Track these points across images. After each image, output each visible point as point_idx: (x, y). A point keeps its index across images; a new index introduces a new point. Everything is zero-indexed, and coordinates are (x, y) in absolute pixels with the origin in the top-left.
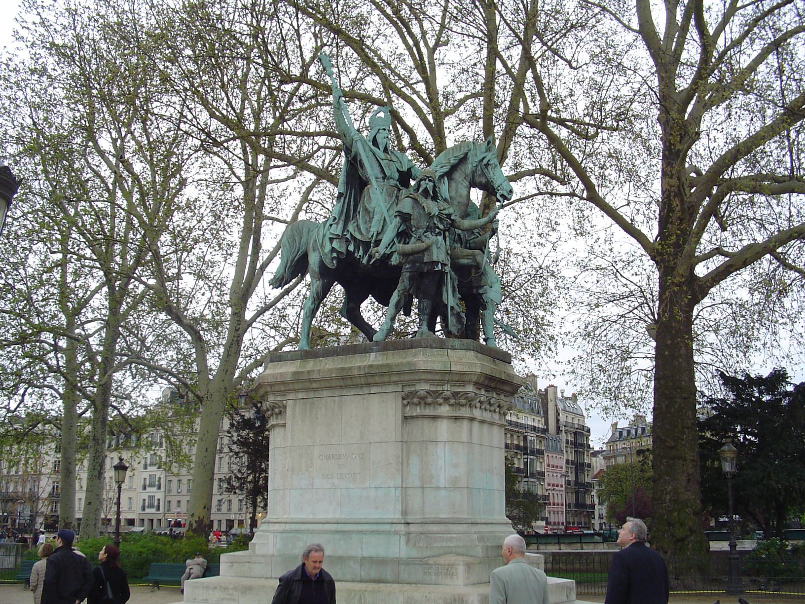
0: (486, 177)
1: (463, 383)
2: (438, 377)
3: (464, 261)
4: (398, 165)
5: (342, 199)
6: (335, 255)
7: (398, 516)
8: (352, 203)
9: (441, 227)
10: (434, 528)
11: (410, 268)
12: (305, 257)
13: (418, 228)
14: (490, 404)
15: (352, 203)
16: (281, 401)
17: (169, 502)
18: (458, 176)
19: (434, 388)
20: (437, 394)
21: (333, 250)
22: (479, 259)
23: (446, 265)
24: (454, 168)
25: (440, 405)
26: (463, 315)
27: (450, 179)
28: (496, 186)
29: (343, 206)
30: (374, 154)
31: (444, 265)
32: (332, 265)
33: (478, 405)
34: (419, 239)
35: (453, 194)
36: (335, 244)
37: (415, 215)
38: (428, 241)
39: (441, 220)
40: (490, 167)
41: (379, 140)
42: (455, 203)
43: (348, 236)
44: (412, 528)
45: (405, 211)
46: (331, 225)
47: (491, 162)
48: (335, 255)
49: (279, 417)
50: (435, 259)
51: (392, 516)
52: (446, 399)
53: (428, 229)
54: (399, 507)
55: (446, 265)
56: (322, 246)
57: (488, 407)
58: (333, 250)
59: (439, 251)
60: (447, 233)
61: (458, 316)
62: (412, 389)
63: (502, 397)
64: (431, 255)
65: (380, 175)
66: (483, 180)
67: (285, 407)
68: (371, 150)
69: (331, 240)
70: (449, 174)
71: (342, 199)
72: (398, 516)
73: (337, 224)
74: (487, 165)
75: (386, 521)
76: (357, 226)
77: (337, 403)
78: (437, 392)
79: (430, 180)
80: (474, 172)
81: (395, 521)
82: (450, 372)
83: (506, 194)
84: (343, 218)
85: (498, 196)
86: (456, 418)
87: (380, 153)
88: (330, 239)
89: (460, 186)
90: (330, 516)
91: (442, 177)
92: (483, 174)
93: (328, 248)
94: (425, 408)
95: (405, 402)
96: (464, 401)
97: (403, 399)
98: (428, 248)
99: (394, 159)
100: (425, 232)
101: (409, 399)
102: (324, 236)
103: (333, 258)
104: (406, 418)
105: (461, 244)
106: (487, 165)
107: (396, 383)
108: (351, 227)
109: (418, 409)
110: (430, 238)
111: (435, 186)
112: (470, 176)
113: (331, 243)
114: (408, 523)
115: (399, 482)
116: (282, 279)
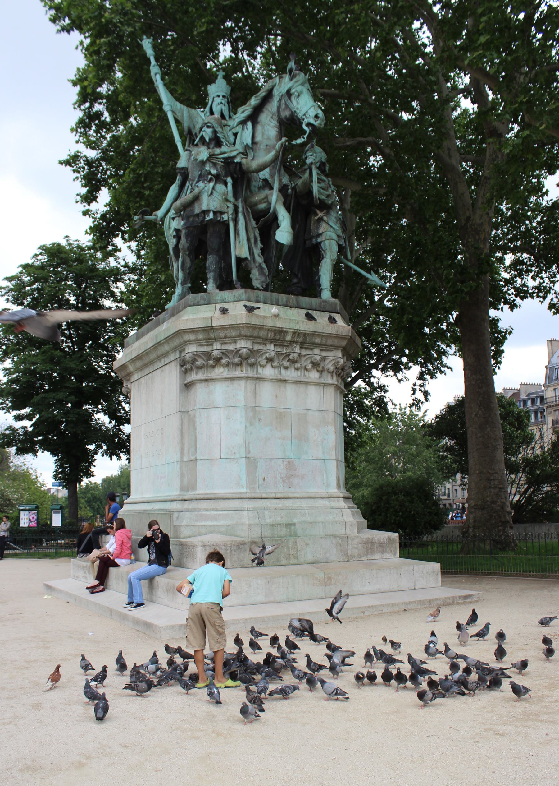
0: (290, 110)
2: (200, 336)
3: (262, 206)
6: (174, 233)
9: (214, 172)
13: (193, 181)
17: (456, 490)
20: (208, 355)
23: (222, 213)
25: (213, 367)
26: (264, 266)
28: (300, 115)
33: (263, 362)
35: (258, 138)
38: (196, 190)
39: (215, 165)
40: (293, 98)
42: (262, 147)
44: (186, 505)
47: (293, 91)
50: (204, 208)
52: (218, 360)
53: (201, 178)
55: (222, 213)
57: (286, 364)
64: (200, 205)
66: (287, 113)
79: (208, 127)
80: (279, 108)
82: (212, 328)
83: (312, 121)
86: (232, 379)
89: (266, 127)
91: (243, 123)
92: (287, 107)
95: (183, 369)
96: (237, 360)
97: (181, 366)
98: (197, 198)
100: (198, 182)
101: (187, 366)
111: (215, 132)
112: (276, 114)
114: (185, 500)
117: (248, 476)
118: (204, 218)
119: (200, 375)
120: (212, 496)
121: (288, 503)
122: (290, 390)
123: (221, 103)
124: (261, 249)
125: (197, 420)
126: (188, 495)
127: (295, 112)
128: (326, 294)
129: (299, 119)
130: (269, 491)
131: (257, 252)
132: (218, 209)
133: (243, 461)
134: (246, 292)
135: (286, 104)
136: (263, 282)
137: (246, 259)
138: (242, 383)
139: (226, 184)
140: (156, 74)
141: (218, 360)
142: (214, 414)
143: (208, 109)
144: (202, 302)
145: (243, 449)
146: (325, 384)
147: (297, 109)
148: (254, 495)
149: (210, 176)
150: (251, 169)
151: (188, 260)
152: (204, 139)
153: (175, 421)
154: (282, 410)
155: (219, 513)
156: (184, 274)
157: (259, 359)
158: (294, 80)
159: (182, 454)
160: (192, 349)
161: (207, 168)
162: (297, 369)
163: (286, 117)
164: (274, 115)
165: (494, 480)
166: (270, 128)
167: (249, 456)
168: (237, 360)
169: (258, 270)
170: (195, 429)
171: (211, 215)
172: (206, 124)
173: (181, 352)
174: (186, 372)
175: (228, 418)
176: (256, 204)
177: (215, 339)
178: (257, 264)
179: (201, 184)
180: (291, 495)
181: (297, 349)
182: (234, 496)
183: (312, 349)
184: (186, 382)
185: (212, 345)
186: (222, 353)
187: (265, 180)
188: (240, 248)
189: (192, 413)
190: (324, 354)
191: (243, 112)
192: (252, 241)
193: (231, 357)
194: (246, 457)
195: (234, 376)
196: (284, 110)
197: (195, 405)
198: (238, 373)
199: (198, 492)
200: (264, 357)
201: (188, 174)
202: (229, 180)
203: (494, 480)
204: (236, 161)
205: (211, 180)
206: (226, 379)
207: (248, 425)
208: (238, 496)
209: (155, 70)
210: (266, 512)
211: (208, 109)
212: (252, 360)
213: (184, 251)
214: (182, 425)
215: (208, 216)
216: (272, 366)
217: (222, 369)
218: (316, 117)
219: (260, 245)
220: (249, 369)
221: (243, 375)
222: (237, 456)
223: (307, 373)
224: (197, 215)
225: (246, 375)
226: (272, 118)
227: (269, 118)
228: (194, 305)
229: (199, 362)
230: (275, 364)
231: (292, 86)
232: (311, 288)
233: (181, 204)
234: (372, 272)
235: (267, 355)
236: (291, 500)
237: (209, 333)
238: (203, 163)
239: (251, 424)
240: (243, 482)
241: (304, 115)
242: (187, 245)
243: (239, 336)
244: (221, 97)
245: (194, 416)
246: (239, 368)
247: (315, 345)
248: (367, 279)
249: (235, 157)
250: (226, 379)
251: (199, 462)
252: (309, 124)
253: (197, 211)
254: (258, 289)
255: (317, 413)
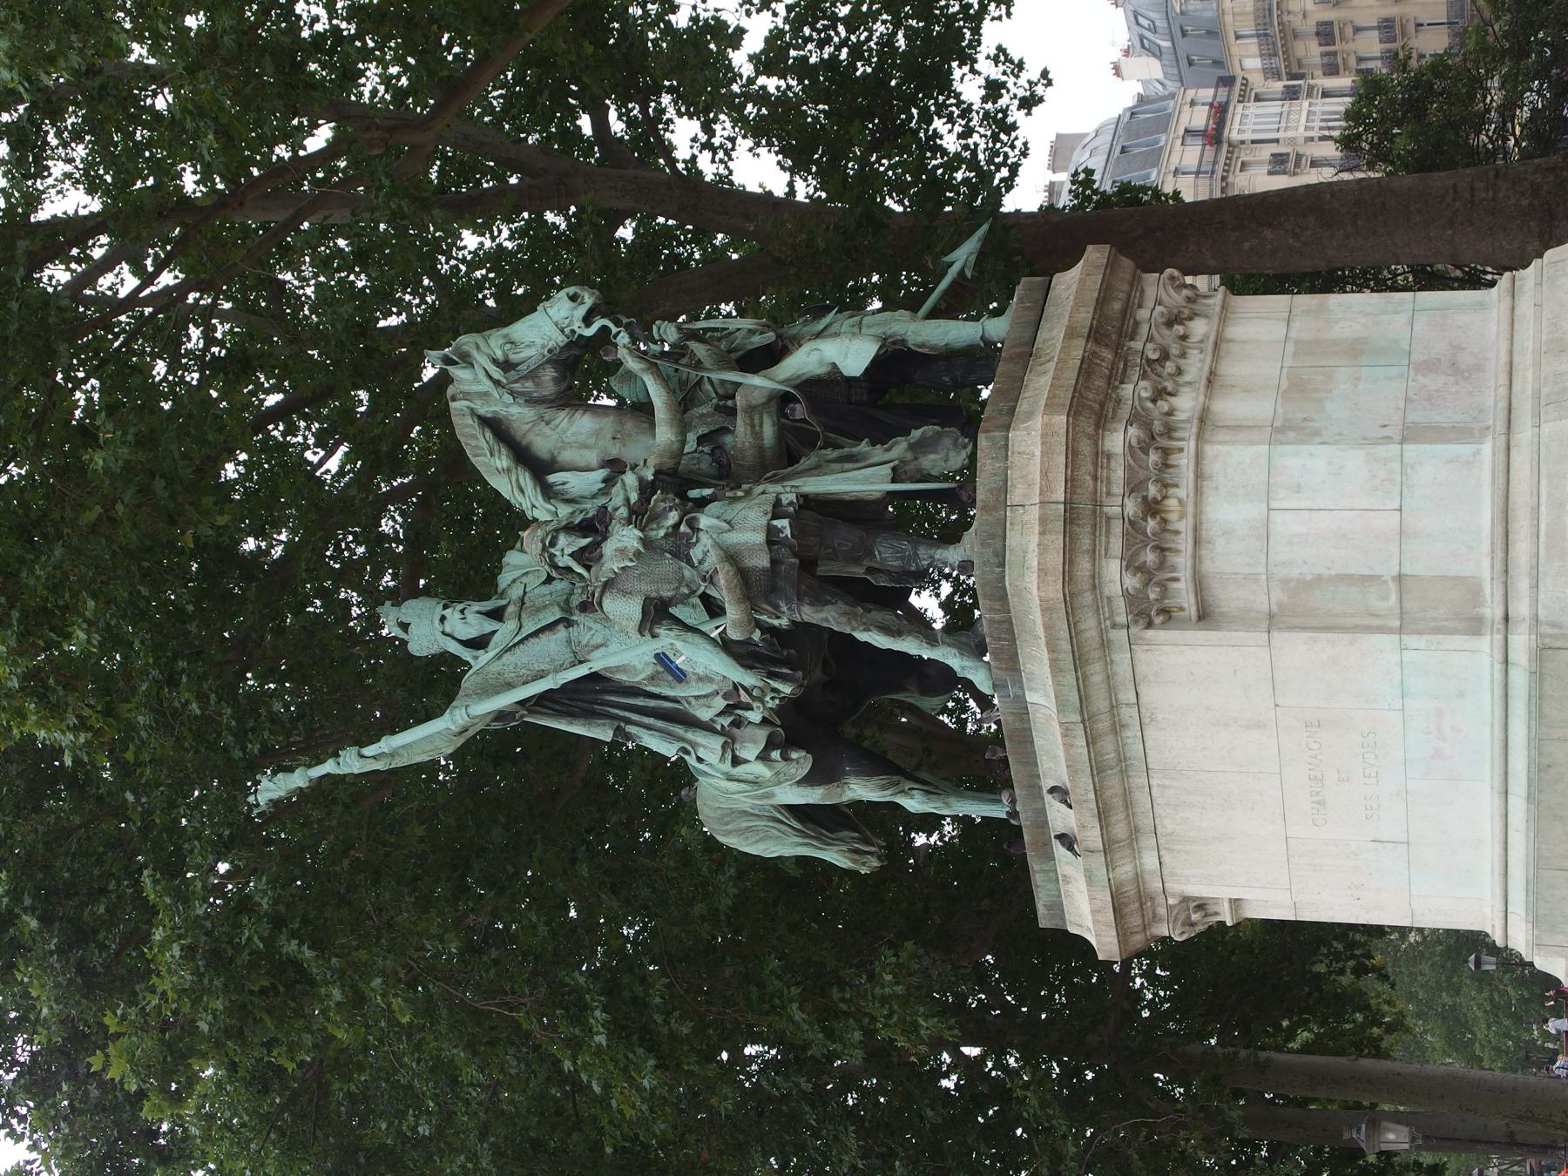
0: (541, 367)
1: (1101, 457)
3: (768, 431)
4: (533, 582)
5: (631, 729)
6: (776, 755)
7: (1485, 647)
8: (640, 702)
9: (673, 517)
10: (1522, 549)
11: (789, 602)
12: (792, 809)
14: (1165, 356)
15: (640, 702)
16: (1169, 908)
18: (542, 443)
19: (1116, 545)
21: (763, 757)
22: (757, 398)
23: (777, 503)
24: (523, 456)
25: (1165, 521)
26: (916, 434)
27: (552, 466)
28: (561, 340)
29: (648, 727)
30: (508, 649)
31: (777, 511)
32: (802, 762)
33: (1163, 406)
34: (710, 579)
35: (592, 457)
36: (749, 751)
37: (648, 588)
38: (713, 560)
39: (656, 518)
40: (514, 358)
41: (470, 632)
43: (726, 721)
44: (1521, 608)
45: (638, 615)
46: (700, 760)
47: (499, 354)
48: (776, 755)
49: (1211, 909)
50: (759, 538)
51: (1487, 660)
54: (1459, 641)
55: (777, 503)
56: (755, 783)
57: (1170, 367)
58: (763, 757)
59: (739, 526)
60: (694, 493)
61: (918, 448)
62: (1120, 604)
63: (1143, 314)
64: (752, 549)
65: (562, 633)
66: (549, 374)
67: (1185, 899)
68: (499, 656)
69: (736, 761)
70: (539, 468)
71: (631, 729)
72: (1485, 647)
73: (694, 745)
74: (506, 365)
75: (1498, 676)
76: (697, 697)
77: (1167, 782)
78: (1125, 534)
79: (553, 544)
80: (531, 401)
81: (1499, 656)
84: (678, 730)
85: (590, 332)
86: (1199, 476)
87: (505, 631)
88: (736, 761)
90: (1488, 804)
91: (548, 492)
92: (533, 375)
93: (760, 769)
94: (1174, 568)
95: (1158, 620)
96: (1154, 457)
97: (1150, 625)
98: (732, 556)
99: (516, 592)
100: (689, 561)
102: (730, 778)
103: (785, 758)
104: (1205, 616)
105: (724, 430)
106: (506, 365)
107: (1105, 645)
108: (705, 715)
109: (1175, 585)
110: (704, 549)
111: (569, 528)
112: (542, 409)
113: (746, 761)
114: (1506, 618)
115: (1387, 641)
116: (856, 851)
117: (1449, 441)
118: (783, 543)
119: (1182, 562)
120: (1499, 530)
121: (1524, 361)
122: (1232, 369)
123: (462, 611)
124: (874, 445)
125: (1294, 573)
126: (1492, 611)
127: (550, 351)
128: (997, 328)
129: (570, 345)
130: (1490, 402)
131: (878, 453)
132: (770, 509)
133: (1410, 449)
134: (987, 431)
135: (525, 378)
136: (955, 443)
137: (894, 469)
138: (1210, 450)
139: (702, 503)
140: (362, 756)
141: (1152, 508)
142: (1285, 525)
143: (466, 654)
144: (999, 543)
145: (1382, 451)
146: (1223, 307)
147: (543, 347)
148: (1500, 427)
149: (683, 528)
150: (676, 446)
151: (878, 616)
152: (583, 549)
153: (1295, 649)
154: (1285, 384)
155: (1543, 499)
156: (909, 633)
157: (1156, 413)
158: (475, 353)
159: (1382, 630)
160: (1115, 577)
161: (662, 533)
162: (1183, 355)
163: (556, 381)
164: (541, 418)
165: (1472, 188)
166: (573, 429)
167: (1398, 438)
168: (1154, 457)
169: (925, 453)
170: (1319, 579)
171: (783, 523)
172: (544, 549)
173: (1114, 626)
174: (1166, 612)
175: (1298, 489)
176: (761, 448)
177: (1097, 504)
178: (909, 456)
179: (696, 553)
180: (1504, 359)
181: (1138, 345)
182: (1501, 467)
183: (1137, 324)
184: (1193, 612)
185: (1108, 519)
186: (1132, 491)
187: (701, 440)
188: (865, 480)
189: (1278, 595)
190: (1150, 303)
191: (522, 491)
192: (850, 466)
193: (1142, 474)
194: (1401, 443)
195: (1192, 468)
196: (537, 385)
197: (1254, 578)
198: (1184, 461)
199: (1486, 575)
200: (1149, 405)
201: (661, 599)
202: (694, 493)
203: (1472, 188)
204: (651, 477)
205: (693, 525)
206: (1198, 490)
207: (1318, 439)
208: (1501, 457)
209: (350, 763)
210: (1545, 391)
211: (466, 654)
212: (1157, 426)
213: (855, 615)
214: (1304, 629)
215: (780, 531)
216: (1170, 394)
217: (1172, 503)
218: (573, 298)
219: (863, 447)
220: (1177, 434)
221: (1192, 443)
222: (1396, 466)
223: (1194, 339)
224: (774, 562)
225: (1193, 438)
226: (548, 423)
227: (547, 430)
228: (1002, 565)
229: (1150, 557)
230: (1170, 386)
231: (489, 356)
232: (979, 361)
233: (739, 602)
234: (947, 259)
235: (1144, 394)
236: (1516, 359)
237: (1077, 518)
238: (646, 542)
239: (1317, 433)
240: (1465, 450)
241: (562, 331)
242: (841, 606)
243: (1096, 445)
244: (448, 612)
245: (1285, 581)
246: (1174, 459)
247: (1127, 312)
248: (961, 272)
249: (641, 480)
250: (1198, 490)
251: (1407, 570)
252: (587, 320)
253: (762, 561)
254: (973, 457)
255: (1296, 324)
